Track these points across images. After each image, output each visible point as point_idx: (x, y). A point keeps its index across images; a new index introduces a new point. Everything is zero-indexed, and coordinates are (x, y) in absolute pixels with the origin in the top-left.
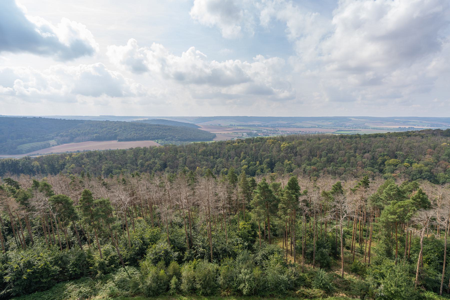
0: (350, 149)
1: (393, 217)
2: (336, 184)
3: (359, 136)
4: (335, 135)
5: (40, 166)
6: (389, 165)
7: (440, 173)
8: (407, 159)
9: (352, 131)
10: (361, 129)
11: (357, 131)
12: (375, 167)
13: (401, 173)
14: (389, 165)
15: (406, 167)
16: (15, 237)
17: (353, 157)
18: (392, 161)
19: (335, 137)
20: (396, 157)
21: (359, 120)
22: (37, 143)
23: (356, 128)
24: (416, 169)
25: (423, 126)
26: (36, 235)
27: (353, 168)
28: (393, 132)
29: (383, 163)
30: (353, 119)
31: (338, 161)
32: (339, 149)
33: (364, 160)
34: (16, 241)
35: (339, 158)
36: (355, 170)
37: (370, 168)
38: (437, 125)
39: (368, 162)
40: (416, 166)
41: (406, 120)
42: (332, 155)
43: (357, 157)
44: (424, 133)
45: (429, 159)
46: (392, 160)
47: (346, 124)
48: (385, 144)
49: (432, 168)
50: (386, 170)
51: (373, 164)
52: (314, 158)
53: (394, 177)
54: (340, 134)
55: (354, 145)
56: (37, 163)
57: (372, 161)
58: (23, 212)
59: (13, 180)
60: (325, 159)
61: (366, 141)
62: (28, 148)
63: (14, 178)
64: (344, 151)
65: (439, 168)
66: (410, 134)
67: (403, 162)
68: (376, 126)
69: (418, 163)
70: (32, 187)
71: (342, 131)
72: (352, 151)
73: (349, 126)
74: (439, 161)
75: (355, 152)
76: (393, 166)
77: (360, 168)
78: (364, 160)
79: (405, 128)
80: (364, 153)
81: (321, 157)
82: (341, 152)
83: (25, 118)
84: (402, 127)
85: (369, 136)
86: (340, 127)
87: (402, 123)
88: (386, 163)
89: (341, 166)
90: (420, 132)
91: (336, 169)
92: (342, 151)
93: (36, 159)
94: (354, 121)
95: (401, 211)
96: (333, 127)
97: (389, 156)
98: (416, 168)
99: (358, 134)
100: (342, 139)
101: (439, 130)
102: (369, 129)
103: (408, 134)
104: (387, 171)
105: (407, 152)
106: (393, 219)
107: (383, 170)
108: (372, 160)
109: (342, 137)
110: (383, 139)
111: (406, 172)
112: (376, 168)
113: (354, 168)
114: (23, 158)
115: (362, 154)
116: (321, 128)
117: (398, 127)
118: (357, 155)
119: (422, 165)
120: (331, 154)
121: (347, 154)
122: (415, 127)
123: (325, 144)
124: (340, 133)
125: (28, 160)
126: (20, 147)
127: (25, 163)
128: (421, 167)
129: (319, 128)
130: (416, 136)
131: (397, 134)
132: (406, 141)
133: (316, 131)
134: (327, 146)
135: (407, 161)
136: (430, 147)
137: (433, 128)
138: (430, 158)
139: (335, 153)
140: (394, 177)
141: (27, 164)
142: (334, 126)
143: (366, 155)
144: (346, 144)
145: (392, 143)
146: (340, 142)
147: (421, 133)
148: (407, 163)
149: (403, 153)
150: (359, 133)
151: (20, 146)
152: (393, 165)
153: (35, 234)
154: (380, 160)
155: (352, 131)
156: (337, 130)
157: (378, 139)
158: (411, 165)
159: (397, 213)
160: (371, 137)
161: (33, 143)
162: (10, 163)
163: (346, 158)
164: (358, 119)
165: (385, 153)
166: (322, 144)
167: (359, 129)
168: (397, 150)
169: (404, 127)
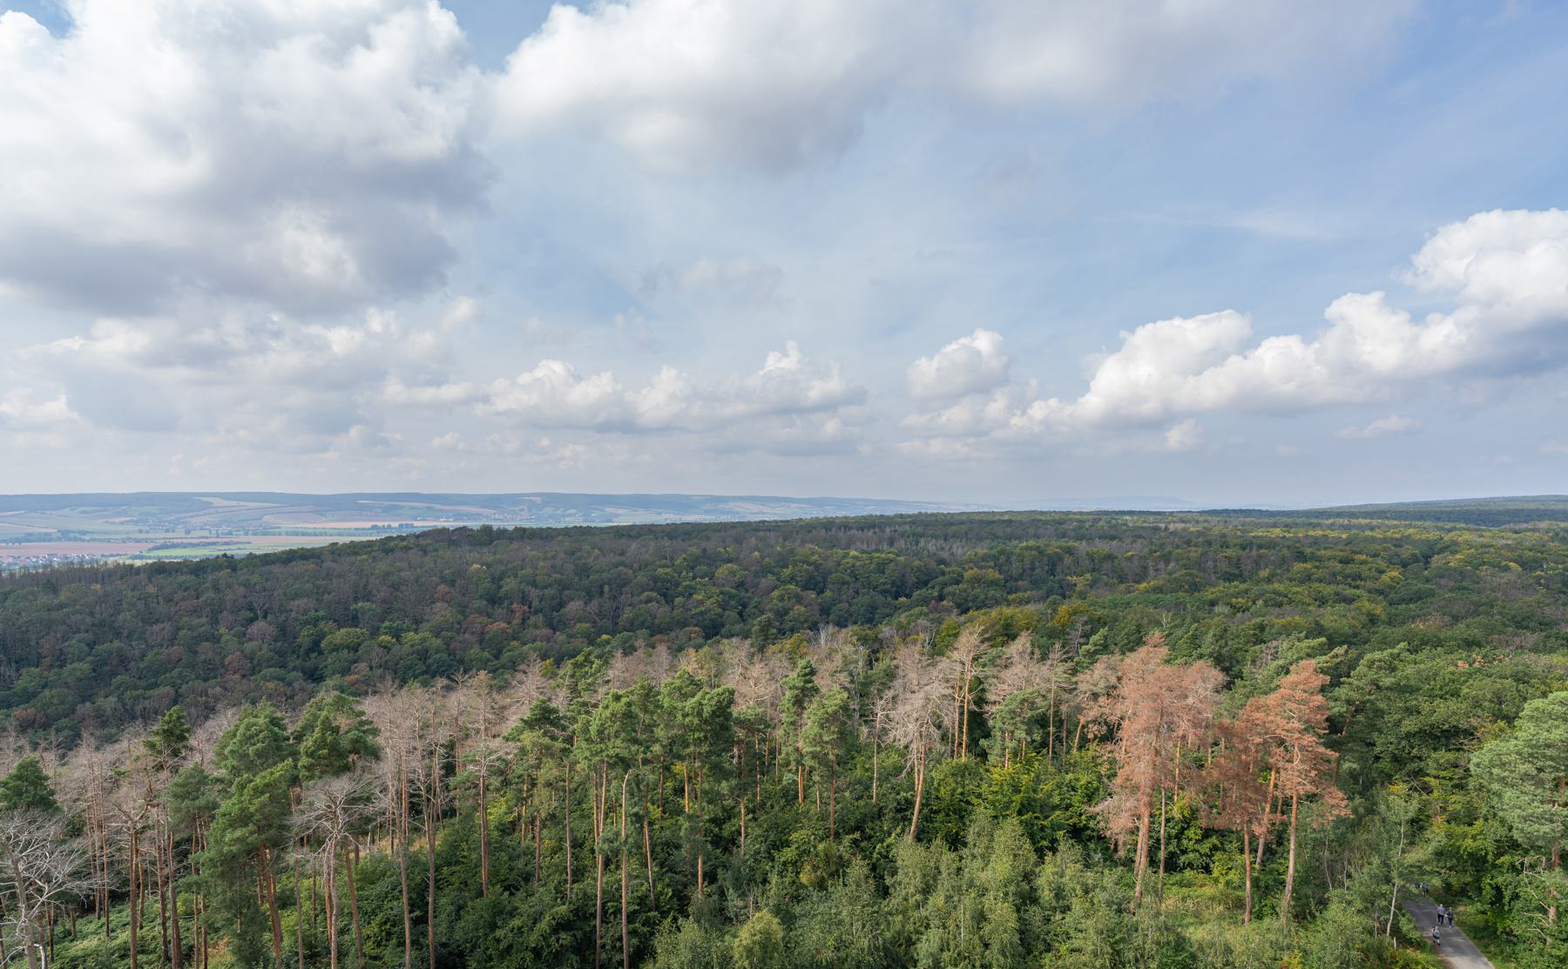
0: (196, 612)
1: (238, 833)
2: (13, 771)
3: (230, 563)
4: (131, 566)
6: (336, 649)
7: (471, 648)
8: (387, 623)
9: (214, 544)
10: (250, 538)
11: (236, 543)
12: (291, 665)
13: (371, 668)
14: (334, 651)
15: (385, 647)
17: (207, 640)
18: (342, 635)
19: (130, 570)
20: (354, 620)
21: (241, 503)
23: (230, 533)
24: (411, 650)
25: (437, 519)
27: (207, 684)
28: (347, 540)
29: (315, 646)
30: (216, 501)
31: (142, 665)
32: (149, 619)
33: (249, 646)
35: (150, 655)
36: (218, 689)
37: (271, 669)
38: (458, 516)
39: (265, 651)
40: (411, 640)
41: (391, 503)
42: (116, 644)
43: (224, 638)
44: (429, 541)
45: (441, 613)
46: (343, 631)
47: (193, 520)
48: (320, 582)
49: (451, 638)
50: (326, 667)
51: (281, 654)
52: (23, 671)
53: (353, 685)
54: (150, 561)
55: (211, 594)
57: (279, 644)
60: (85, 666)
61: (255, 578)
64: (167, 626)
65: (467, 636)
66: (392, 544)
67: (375, 632)
68: (301, 526)
69: (416, 631)
71: (174, 546)
72: (204, 620)
73: (202, 529)
74: (466, 617)
75: (215, 621)
76: (346, 651)
77: (237, 676)
78: (249, 646)
79: (389, 526)
80: (252, 621)
81: (61, 660)
82: (156, 628)
84: (380, 524)
85: (267, 560)
86: (167, 531)
87: (380, 510)
88: (323, 645)
89: (156, 685)
90: (418, 537)
91: (137, 698)
92: (160, 626)
94: (220, 510)
95: (264, 806)
96: (133, 536)
97: (335, 621)
98: (412, 646)
99: (225, 555)
100: (160, 578)
101: (464, 528)
102: (280, 534)
103: (387, 547)
104: (327, 672)
105: (384, 601)
106: (238, 840)
107: (316, 668)
108: (276, 641)
109: (160, 569)
110: (311, 566)
111: (386, 662)
112: (294, 669)
113: (212, 682)
115: (242, 626)
116: (76, 539)
117: (369, 525)
118: (222, 630)
119: (427, 634)
120: (111, 642)
121: (182, 633)
122: (416, 524)
123: (77, 607)
124: (154, 558)
128: (424, 640)
129: (70, 540)
130: (407, 549)
131: (355, 547)
132: (382, 566)
133: (55, 555)
134: (92, 614)
135: (385, 628)
136: (443, 580)
137: (452, 524)
138: (445, 610)
139: (129, 637)
140: (353, 685)
142: (141, 531)
143: (259, 626)
144: (177, 597)
145: (339, 576)
146: (151, 589)
147: (422, 542)
148: (386, 634)
149: (374, 606)
150: (229, 553)
152: (348, 647)
154: (305, 636)
155: (214, 544)
156: (151, 545)
157: (297, 567)
158: (397, 640)
159: (252, 815)
160: (273, 563)
163: (176, 650)
164: (235, 503)
165: (321, 613)
166: (61, 606)
167: (243, 538)
168: (356, 600)
169: (386, 524)
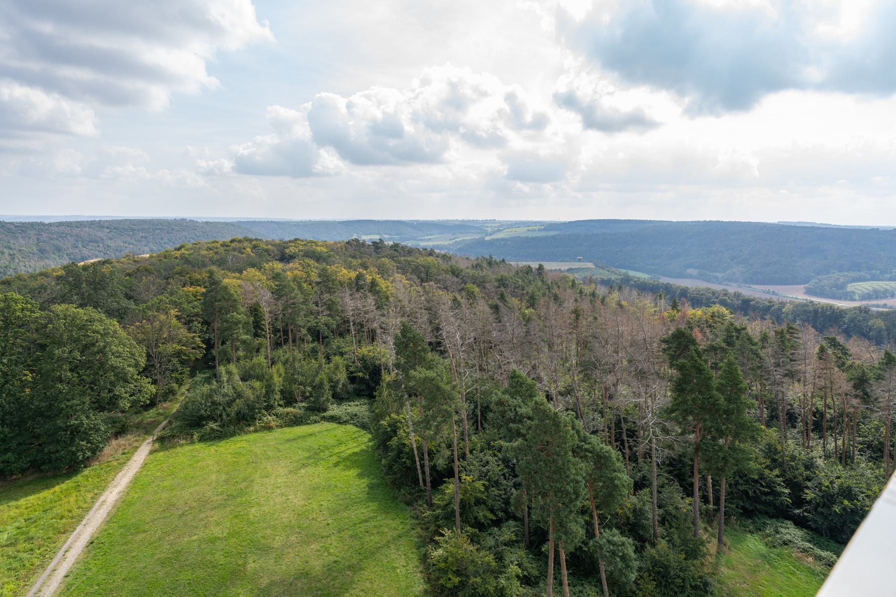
5: (886, 330)
16: (824, 440)
22: (887, 283)
26: (862, 455)
34: (824, 447)
56: (880, 323)
58: (855, 402)
59: (839, 343)
62: (867, 291)
63: (841, 339)
70: (879, 363)
83: (875, 231)
93: (880, 315)
114: (855, 308)
125: (863, 314)
126: (850, 287)
127: (856, 318)
141: (859, 321)
151: (853, 284)
153: (859, 451)
161: (880, 283)
162: (828, 313)
